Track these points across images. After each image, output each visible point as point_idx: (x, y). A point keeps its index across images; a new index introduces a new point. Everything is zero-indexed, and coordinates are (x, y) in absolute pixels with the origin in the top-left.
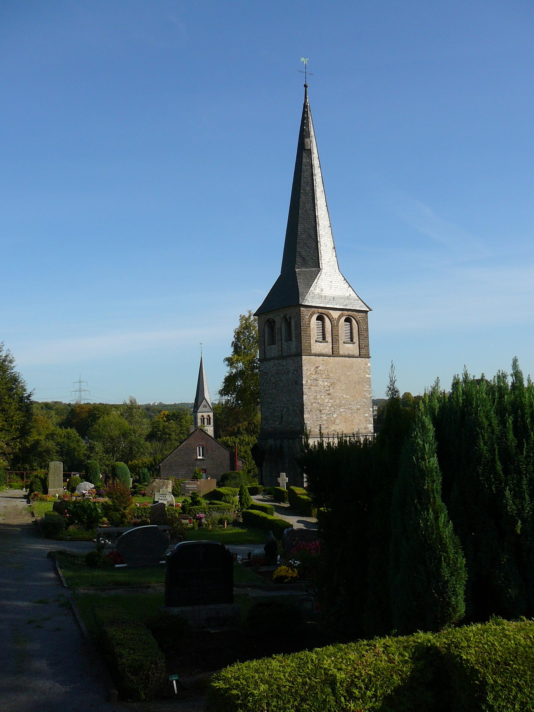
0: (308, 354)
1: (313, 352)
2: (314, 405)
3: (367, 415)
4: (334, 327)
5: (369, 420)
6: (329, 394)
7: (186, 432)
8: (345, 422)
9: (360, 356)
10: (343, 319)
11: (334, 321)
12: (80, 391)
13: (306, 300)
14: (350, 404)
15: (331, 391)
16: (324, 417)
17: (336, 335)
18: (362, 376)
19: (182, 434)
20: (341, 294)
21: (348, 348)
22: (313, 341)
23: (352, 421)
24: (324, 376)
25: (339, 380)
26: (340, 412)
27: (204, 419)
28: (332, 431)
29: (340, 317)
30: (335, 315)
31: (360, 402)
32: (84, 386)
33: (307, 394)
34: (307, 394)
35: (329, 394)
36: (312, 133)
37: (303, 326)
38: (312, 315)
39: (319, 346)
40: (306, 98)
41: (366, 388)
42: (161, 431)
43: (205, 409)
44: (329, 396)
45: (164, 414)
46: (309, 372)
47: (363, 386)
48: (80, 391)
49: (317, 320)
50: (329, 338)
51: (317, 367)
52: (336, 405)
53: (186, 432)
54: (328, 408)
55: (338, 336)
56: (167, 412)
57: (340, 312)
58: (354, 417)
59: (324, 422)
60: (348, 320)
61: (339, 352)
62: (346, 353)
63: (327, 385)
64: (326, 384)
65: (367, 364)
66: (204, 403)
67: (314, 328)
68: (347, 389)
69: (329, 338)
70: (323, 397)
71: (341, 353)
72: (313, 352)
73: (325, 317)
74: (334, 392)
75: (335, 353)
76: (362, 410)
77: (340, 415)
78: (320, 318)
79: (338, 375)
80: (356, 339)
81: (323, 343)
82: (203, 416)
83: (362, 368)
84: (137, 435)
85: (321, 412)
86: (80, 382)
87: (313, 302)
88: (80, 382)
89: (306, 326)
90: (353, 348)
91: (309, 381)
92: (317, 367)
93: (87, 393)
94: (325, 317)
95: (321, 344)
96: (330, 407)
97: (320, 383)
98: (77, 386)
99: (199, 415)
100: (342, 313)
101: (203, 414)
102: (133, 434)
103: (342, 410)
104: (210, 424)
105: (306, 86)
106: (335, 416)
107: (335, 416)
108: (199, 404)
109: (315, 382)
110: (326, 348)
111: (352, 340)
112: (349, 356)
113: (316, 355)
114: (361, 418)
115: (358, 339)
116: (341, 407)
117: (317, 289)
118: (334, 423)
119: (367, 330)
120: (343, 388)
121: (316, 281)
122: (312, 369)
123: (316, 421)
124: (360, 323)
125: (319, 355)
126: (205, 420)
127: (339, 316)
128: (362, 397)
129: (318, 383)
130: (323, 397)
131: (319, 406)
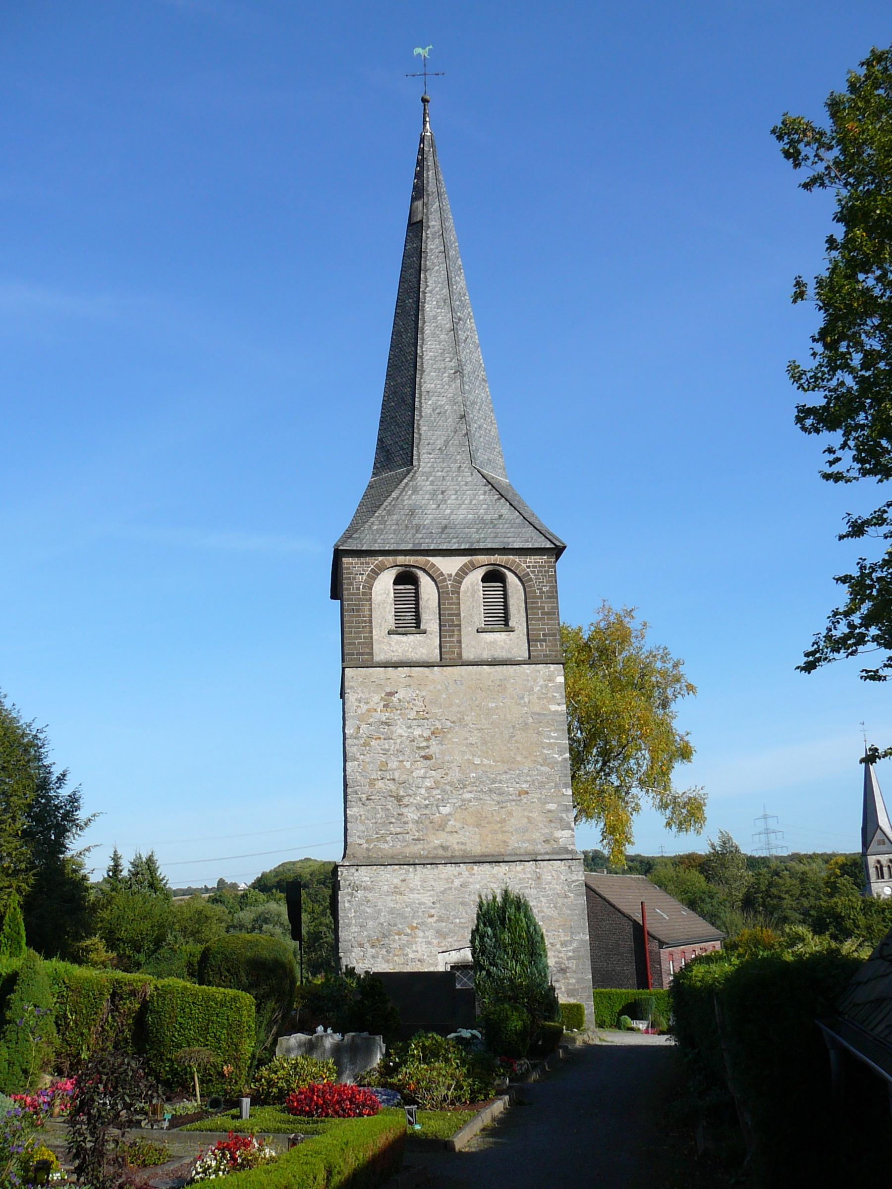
0: (361, 664)
1: (379, 657)
2: (380, 784)
3: (552, 806)
4: (448, 595)
5: (562, 819)
6: (426, 758)
7: (813, 892)
8: (478, 826)
9: (531, 660)
10: (480, 573)
11: (444, 580)
12: (767, 832)
13: (355, 539)
14: (494, 782)
15: (435, 748)
16: (411, 815)
17: (450, 615)
18: (537, 709)
19: (807, 896)
20: (470, 516)
21: (493, 643)
22: (379, 633)
23: (503, 821)
24: (413, 715)
25: (460, 722)
26: (463, 800)
27: (881, 867)
28: (435, 848)
29: (464, 572)
30: (449, 566)
31: (528, 775)
32: (772, 824)
33: (356, 759)
34: (356, 759)
35: (426, 758)
36: (431, 188)
37: (349, 600)
38: (375, 573)
39: (397, 642)
40: (425, 122)
41: (550, 737)
42: (762, 892)
43: (882, 848)
44: (428, 762)
45: (837, 863)
46: (364, 708)
47: (539, 733)
48: (767, 832)
49: (395, 583)
50: (430, 620)
51: (391, 694)
52: (450, 784)
53: (813, 892)
54: (423, 791)
55: (459, 615)
56: (841, 860)
57: (465, 559)
58: (510, 814)
59: (410, 825)
60: (494, 576)
61: (460, 655)
62: (486, 655)
63: (421, 736)
64: (417, 732)
65: (551, 679)
66: (878, 836)
67: (384, 602)
68: (485, 743)
69: (430, 620)
70: (408, 765)
71: (468, 654)
72: (379, 657)
73: (420, 573)
74: (443, 753)
75: (449, 657)
76: (535, 796)
77: (464, 806)
78: (406, 578)
79: (455, 709)
80: (517, 618)
81: (411, 637)
82: (879, 862)
83: (537, 689)
84: (715, 902)
85: (399, 799)
86: (765, 817)
87: (375, 542)
88: (765, 817)
89: (360, 600)
90: (513, 643)
91: (364, 727)
92: (391, 694)
93: (779, 835)
94: (420, 573)
95: (404, 638)
96: (429, 789)
97: (400, 731)
98: (761, 824)
99: (872, 860)
100: (471, 562)
101: (879, 857)
102: (708, 900)
103: (467, 796)
104: (883, 878)
105: (424, 101)
106: (445, 810)
107: (445, 810)
108: (869, 839)
109: (384, 729)
110: (424, 646)
111: (506, 620)
112: (494, 663)
113: (386, 665)
114: (534, 815)
115: (525, 619)
116: (465, 786)
117: (397, 510)
118: (442, 827)
119: (553, 595)
120: (472, 740)
121: (394, 495)
122: (376, 698)
123: (384, 824)
124: (531, 580)
125: (396, 665)
126: (885, 869)
127: (461, 569)
128: (535, 762)
129: (392, 733)
130: (408, 765)
131: (392, 786)
